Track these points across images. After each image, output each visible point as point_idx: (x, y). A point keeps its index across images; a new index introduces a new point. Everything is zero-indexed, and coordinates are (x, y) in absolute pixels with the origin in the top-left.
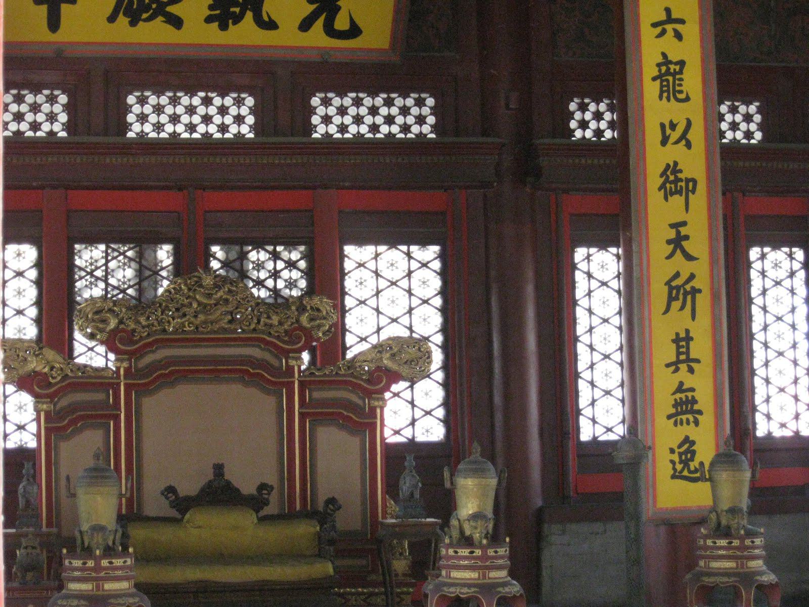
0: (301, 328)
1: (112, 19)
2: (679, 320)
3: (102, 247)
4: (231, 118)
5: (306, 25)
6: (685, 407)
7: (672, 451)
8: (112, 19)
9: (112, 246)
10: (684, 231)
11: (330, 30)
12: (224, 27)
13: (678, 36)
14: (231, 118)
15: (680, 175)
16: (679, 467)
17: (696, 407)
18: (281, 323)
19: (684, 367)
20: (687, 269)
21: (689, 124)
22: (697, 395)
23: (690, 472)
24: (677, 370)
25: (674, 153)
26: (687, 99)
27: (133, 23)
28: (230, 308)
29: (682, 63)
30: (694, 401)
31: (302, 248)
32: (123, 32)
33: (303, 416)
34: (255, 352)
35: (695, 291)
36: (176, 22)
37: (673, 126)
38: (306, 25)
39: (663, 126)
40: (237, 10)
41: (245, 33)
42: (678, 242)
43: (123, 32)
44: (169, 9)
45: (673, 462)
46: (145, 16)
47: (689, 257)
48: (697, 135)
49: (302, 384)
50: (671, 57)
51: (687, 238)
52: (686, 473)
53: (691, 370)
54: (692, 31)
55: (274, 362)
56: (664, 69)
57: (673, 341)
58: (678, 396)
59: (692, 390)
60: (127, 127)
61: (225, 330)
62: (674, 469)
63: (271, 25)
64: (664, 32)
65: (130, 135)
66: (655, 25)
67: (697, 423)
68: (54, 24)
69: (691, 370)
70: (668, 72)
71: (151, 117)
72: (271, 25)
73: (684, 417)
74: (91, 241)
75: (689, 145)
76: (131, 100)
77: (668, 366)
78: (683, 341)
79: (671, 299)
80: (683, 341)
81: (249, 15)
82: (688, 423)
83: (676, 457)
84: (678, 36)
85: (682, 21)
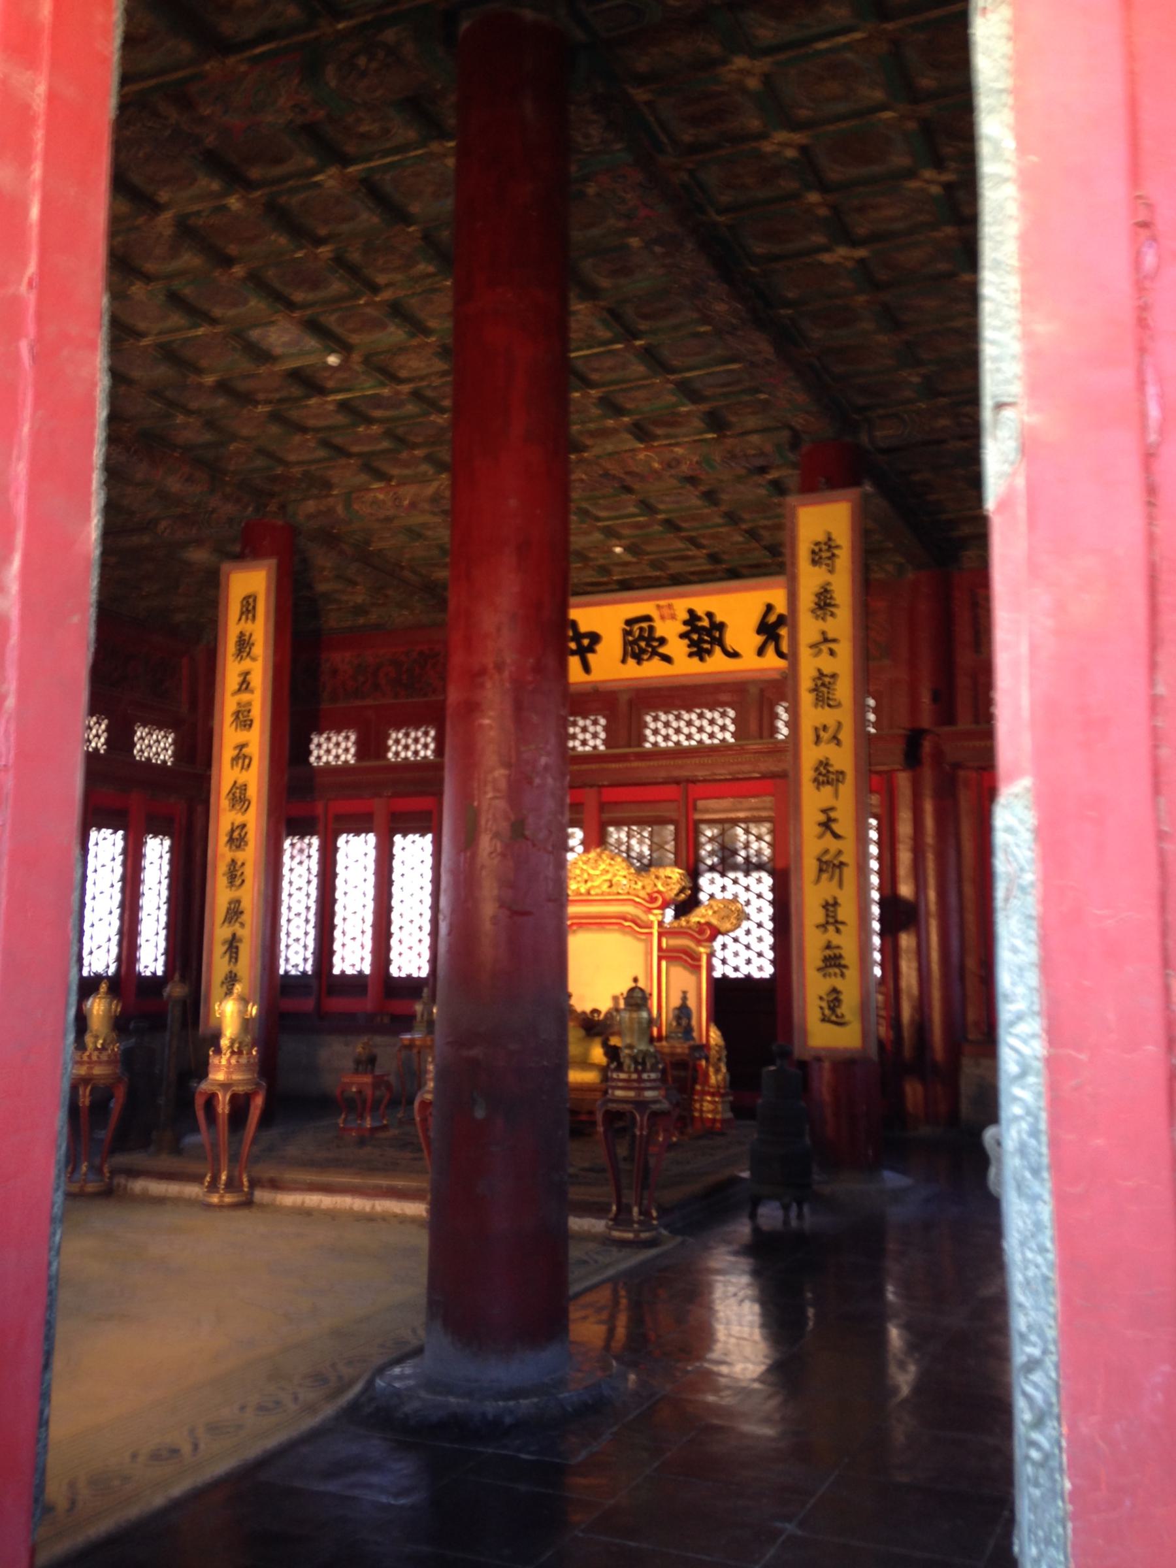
0: (659, 892)
1: (624, 661)
2: (826, 889)
3: (626, 829)
4: (715, 728)
5: (761, 652)
6: (832, 961)
7: (821, 998)
8: (624, 661)
9: (635, 828)
10: (833, 815)
11: (781, 654)
12: (702, 659)
13: (832, 653)
14: (715, 728)
15: (831, 769)
16: (827, 1012)
17: (843, 962)
18: (643, 887)
19: (831, 928)
20: (833, 845)
21: (839, 725)
22: (843, 952)
23: (837, 1016)
24: (826, 930)
25: (827, 750)
26: (839, 705)
27: (639, 661)
28: (608, 877)
29: (834, 676)
30: (841, 957)
31: (768, 825)
32: (633, 671)
33: (660, 959)
34: (629, 909)
35: (842, 864)
36: (667, 659)
37: (825, 728)
38: (761, 652)
39: (816, 729)
40: (706, 646)
41: (717, 663)
42: (827, 825)
43: (633, 671)
44: (662, 650)
45: (821, 1008)
46: (645, 657)
47: (836, 836)
48: (847, 736)
49: (660, 935)
50: (825, 672)
51: (835, 820)
52: (834, 1018)
53: (838, 931)
54: (845, 649)
55: (643, 916)
56: (819, 682)
57: (824, 907)
58: (828, 952)
59: (838, 947)
60: (644, 739)
61: (609, 894)
62: (823, 1014)
63: (734, 655)
64: (820, 651)
65: (648, 745)
66: (812, 646)
67: (843, 975)
68: (587, 668)
69: (838, 931)
70: (823, 685)
71: (665, 731)
72: (734, 655)
73: (832, 970)
74: (618, 824)
75: (839, 743)
76: (649, 719)
77: (818, 927)
78: (830, 907)
79: (821, 870)
80: (830, 907)
81: (718, 649)
82: (835, 975)
83: (824, 1004)
84: (832, 653)
85: (834, 641)
